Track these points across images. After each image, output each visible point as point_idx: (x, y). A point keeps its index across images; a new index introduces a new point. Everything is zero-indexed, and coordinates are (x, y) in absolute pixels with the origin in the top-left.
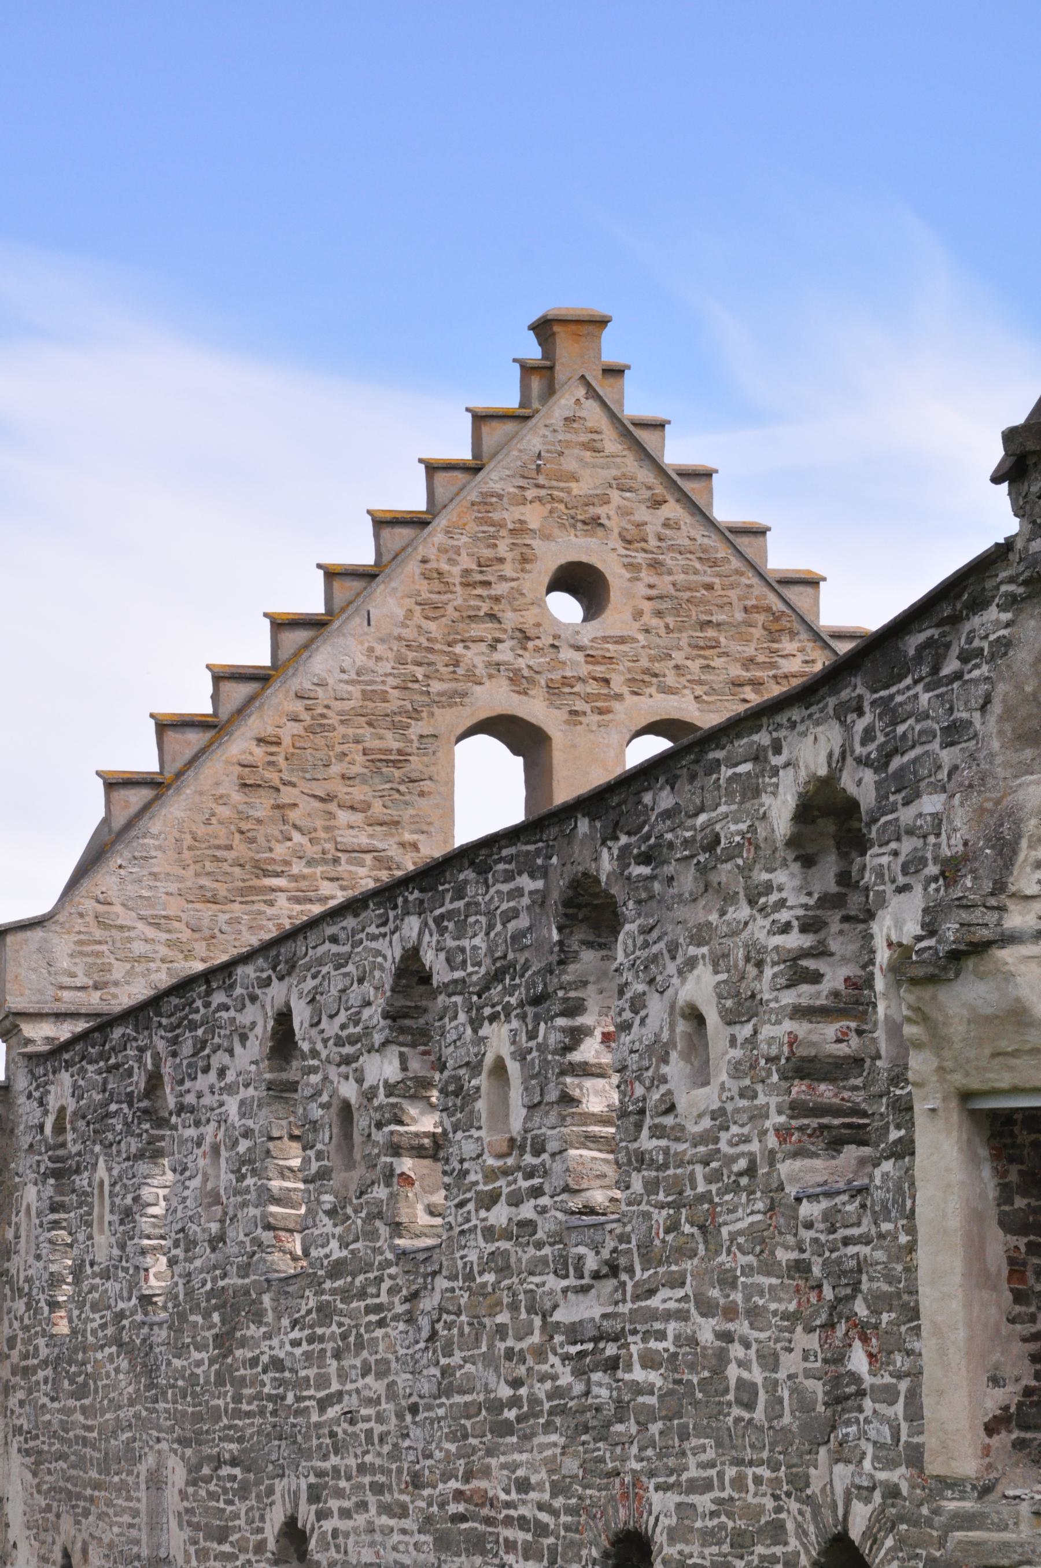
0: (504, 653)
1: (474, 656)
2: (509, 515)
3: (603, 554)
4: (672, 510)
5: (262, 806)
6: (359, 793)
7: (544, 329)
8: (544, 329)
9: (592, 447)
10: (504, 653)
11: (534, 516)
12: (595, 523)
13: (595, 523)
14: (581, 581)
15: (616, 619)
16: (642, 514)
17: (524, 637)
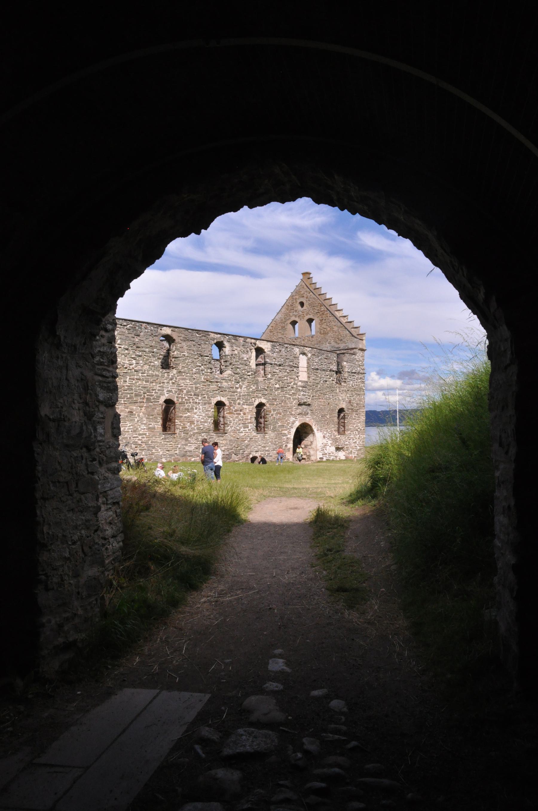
0: (294, 313)
1: (291, 314)
2: (294, 297)
4: (311, 293)
5: (272, 334)
6: (280, 331)
9: (303, 288)
10: (294, 313)
11: (297, 297)
12: (303, 297)
13: (303, 297)
14: (302, 304)
15: (305, 307)
16: (308, 294)
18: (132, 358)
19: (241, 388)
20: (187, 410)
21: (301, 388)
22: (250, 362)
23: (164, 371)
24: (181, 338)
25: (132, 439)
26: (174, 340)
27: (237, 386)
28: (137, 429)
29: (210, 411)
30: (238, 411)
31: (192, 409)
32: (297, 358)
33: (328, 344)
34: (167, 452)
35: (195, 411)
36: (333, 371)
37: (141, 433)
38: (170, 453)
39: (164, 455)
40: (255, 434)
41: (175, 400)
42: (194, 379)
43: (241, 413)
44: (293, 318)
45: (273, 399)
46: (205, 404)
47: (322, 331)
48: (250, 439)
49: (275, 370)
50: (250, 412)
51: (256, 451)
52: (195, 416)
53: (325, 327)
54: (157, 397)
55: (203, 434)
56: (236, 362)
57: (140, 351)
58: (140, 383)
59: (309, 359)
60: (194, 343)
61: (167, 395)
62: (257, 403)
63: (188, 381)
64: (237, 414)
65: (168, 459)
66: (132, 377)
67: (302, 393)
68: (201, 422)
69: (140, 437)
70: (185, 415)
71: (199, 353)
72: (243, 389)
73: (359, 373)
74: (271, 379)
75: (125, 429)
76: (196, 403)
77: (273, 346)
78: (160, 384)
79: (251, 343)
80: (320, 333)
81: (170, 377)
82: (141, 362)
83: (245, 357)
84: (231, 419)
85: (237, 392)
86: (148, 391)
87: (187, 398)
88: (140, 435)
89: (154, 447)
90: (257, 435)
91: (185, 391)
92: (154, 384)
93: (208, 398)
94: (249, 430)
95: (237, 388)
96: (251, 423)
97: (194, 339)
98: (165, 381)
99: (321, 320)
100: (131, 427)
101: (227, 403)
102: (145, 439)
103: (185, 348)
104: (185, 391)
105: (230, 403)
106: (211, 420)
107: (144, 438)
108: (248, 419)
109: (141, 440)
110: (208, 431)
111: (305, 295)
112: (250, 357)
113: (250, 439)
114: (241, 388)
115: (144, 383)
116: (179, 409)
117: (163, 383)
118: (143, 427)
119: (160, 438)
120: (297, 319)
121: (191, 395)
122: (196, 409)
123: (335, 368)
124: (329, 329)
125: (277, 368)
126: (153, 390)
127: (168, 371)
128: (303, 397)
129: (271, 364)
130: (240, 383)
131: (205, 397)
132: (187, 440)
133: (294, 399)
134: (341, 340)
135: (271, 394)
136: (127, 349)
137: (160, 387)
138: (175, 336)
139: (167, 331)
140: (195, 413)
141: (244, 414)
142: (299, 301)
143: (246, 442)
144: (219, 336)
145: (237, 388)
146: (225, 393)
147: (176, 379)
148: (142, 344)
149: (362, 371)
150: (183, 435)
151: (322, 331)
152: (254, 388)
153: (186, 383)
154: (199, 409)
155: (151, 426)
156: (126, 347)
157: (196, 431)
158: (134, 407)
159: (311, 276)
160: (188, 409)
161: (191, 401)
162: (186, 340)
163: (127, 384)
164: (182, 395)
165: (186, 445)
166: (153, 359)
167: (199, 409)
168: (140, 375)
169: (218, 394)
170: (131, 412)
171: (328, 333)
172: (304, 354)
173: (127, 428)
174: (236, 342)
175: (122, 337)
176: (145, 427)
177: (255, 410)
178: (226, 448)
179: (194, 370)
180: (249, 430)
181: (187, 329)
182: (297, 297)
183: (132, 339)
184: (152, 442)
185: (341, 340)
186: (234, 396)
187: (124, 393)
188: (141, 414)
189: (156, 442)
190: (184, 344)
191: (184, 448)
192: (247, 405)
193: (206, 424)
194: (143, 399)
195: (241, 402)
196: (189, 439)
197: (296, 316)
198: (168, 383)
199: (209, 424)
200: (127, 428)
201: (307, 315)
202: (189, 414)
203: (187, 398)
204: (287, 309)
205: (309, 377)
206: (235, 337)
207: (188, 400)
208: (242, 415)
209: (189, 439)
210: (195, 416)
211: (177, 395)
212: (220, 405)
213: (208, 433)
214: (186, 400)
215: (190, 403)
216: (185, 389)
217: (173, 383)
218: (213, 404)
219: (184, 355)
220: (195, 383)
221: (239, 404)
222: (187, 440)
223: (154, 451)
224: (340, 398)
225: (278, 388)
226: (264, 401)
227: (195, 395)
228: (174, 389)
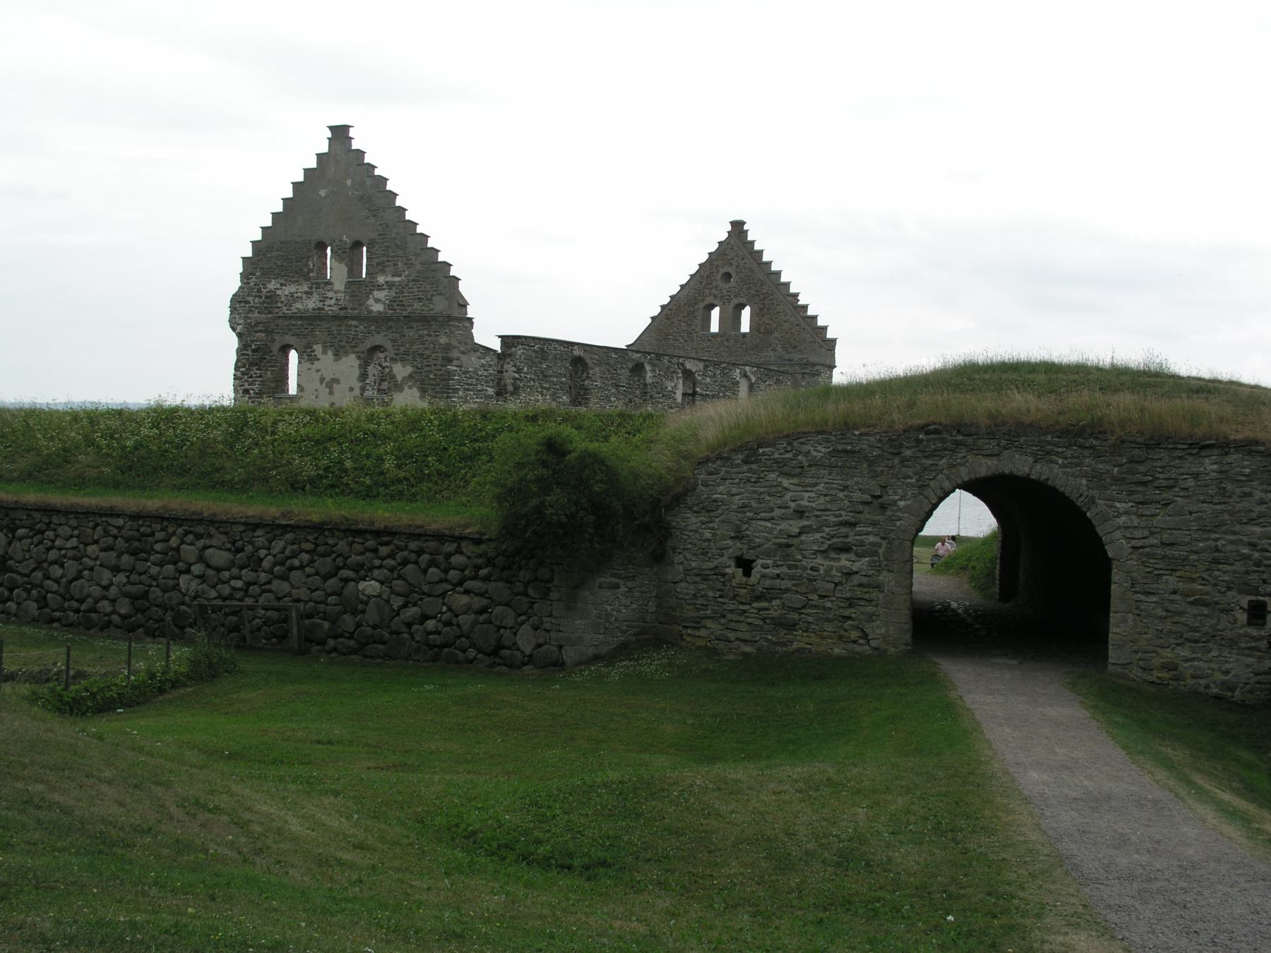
1: (707, 291)
7: (734, 224)
8: (734, 224)
11: (720, 263)
17: (716, 287)
33: (771, 353)
44: (709, 300)
47: (762, 329)
77: (706, 367)
99: (761, 310)
120: (715, 302)
139: (577, 353)
142: (722, 271)
151: (762, 329)
159: (745, 227)
162: (600, 363)
171: (771, 333)
172: (745, 375)
182: (720, 263)
197: (715, 297)
204: (701, 283)
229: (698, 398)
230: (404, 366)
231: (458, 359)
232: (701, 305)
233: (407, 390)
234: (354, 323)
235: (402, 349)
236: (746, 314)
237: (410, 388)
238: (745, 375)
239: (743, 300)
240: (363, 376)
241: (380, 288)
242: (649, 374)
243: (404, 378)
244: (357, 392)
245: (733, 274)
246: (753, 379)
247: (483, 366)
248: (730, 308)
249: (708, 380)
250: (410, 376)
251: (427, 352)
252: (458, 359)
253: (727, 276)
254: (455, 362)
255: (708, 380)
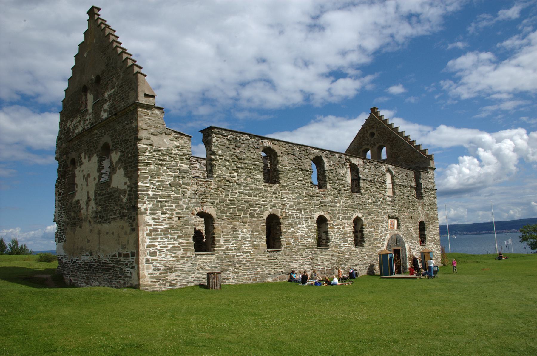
1: (363, 143)
3: (374, 131)
11: (368, 128)
15: (375, 137)
18: (234, 170)
19: (340, 203)
20: (291, 225)
21: (389, 203)
22: (346, 177)
23: (267, 185)
24: (283, 151)
25: (236, 257)
26: (276, 153)
27: (336, 201)
28: (241, 247)
29: (313, 226)
30: (338, 225)
31: (296, 224)
32: (384, 174)
34: (273, 271)
35: (299, 226)
36: (413, 187)
37: (245, 250)
38: (275, 271)
39: (270, 274)
40: (354, 248)
41: (279, 215)
42: (296, 193)
43: (341, 227)
44: (365, 147)
45: (368, 213)
46: (308, 218)
48: (350, 253)
49: (367, 186)
50: (349, 227)
51: (356, 265)
52: (299, 232)
53: (395, 151)
54: (261, 211)
55: (307, 250)
56: (334, 177)
57: (242, 163)
58: (243, 197)
59: (392, 177)
60: (294, 157)
61: (270, 210)
62: (354, 217)
63: (291, 195)
64: (337, 228)
65: (274, 278)
66: (234, 191)
67: (390, 207)
68: (305, 237)
69: (244, 256)
70: (289, 231)
71: (300, 167)
72: (341, 204)
73: (432, 190)
74: (365, 194)
75: (228, 247)
76: (299, 218)
78: (263, 198)
79: (346, 160)
80: (392, 157)
81: (273, 191)
82: (243, 175)
83: (342, 172)
84: (332, 234)
85: (336, 207)
86: (251, 206)
87: (290, 213)
88: (244, 253)
89: (259, 266)
90: (355, 249)
91: (288, 206)
92: (257, 198)
93: (311, 212)
94: (348, 244)
95: (336, 203)
96: (350, 237)
97: (295, 153)
98: (269, 195)
99: (392, 146)
100: (235, 245)
101: (328, 217)
102: (250, 257)
103: (286, 162)
104: (288, 206)
105: (331, 218)
106: (314, 235)
107: (248, 256)
108: (347, 233)
109: (246, 258)
110: (311, 247)
111: (375, 127)
112: (346, 173)
113: (350, 253)
114: (340, 203)
115: (247, 197)
116: (283, 224)
117: (267, 197)
118: (247, 244)
119: (264, 255)
120: (369, 147)
121: (294, 210)
122: (300, 224)
123: (414, 185)
124: (399, 153)
125: (369, 183)
126: (256, 204)
127: (270, 185)
128: (391, 211)
129: (364, 180)
130: (339, 198)
131: (307, 212)
132: (291, 256)
133: (385, 213)
134: (412, 161)
135: (366, 209)
136: (228, 161)
137: (263, 201)
138: (276, 148)
140: (299, 229)
141: (344, 228)
142: (369, 132)
143: (347, 256)
144: (317, 151)
145: (336, 203)
146: (325, 208)
147: (279, 193)
148: (244, 156)
149: (434, 188)
150: (287, 251)
151: (393, 156)
152: (350, 203)
153: (289, 198)
154: (303, 224)
155: (255, 243)
156: (227, 158)
157: (301, 247)
158: (238, 223)
160: (292, 224)
161: (295, 216)
163: (230, 198)
164: (286, 209)
165: (291, 262)
166: (254, 172)
167: (303, 224)
168: (243, 188)
169: (320, 208)
170: (234, 230)
172: (388, 171)
173: (230, 246)
174: (333, 158)
175: (224, 148)
176: (249, 245)
177: (353, 224)
178: (329, 263)
179: (296, 184)
180: (348, 244)
181: (288, 143)
182: (368, 128)
183: (233, 150)
184: (256, 260)
185: (412, 161)
186: (333, 210)
187: (226, 207)
188: (245, 230)
189: (261, 260)
190: (285, 157)
191: (289, 265)
192: (345, 219)
193: (309, 240)
194: (246, 214)
195: (341, 217)
196: (294, 256)
197: (367, 145)
198: (271, 197)
199: (312, 240)
200: (230, 246)
201: (378, 143)
202: (292, 229)
203: (290, 213)
204: (360, 140)
205: (394, 193)
206: (332, 153)
207: (292, 215)
208: (342, 229)
209: (294, 256)
210: (299, 232)
211: (280, 210)
212: (321, 221)
213: (312, 248)
214: (289, 215)
215: (294, 218)
216: (288, 204)
217: (276, 197)
218: (315, 219)
219: (286, 169)
220: (297, 198)
221: (339, 218)
222: (291, 256)
223: (259, 270)
224: (420, 212)
225: (371, 203)
226: (360, 215)
227: (298, 210)
228: (277, 202)
229: (362, 181)
230: (116, 153)
231: (148, 139)
232: (361, 150)
233: (118, 171)
234: (96, 132)
235: (115, 140)
236: (384, 151)
237: (119, 169)
238: (388, 171)
239: (382, 144)
240: (101, 167)
241: (105, 101)
242: (326, 164)
243: (117, 163)
244: (97, 181)
245: (375, 132)
246: (394, 172)
247: (176, 147)
248: (376, 149)
249: (367, 171)
250: (120, 159)
251: (127, 138)
252: (148, 139)
253: (372, 134)
254: (144, 141)
255: (367, 171)
